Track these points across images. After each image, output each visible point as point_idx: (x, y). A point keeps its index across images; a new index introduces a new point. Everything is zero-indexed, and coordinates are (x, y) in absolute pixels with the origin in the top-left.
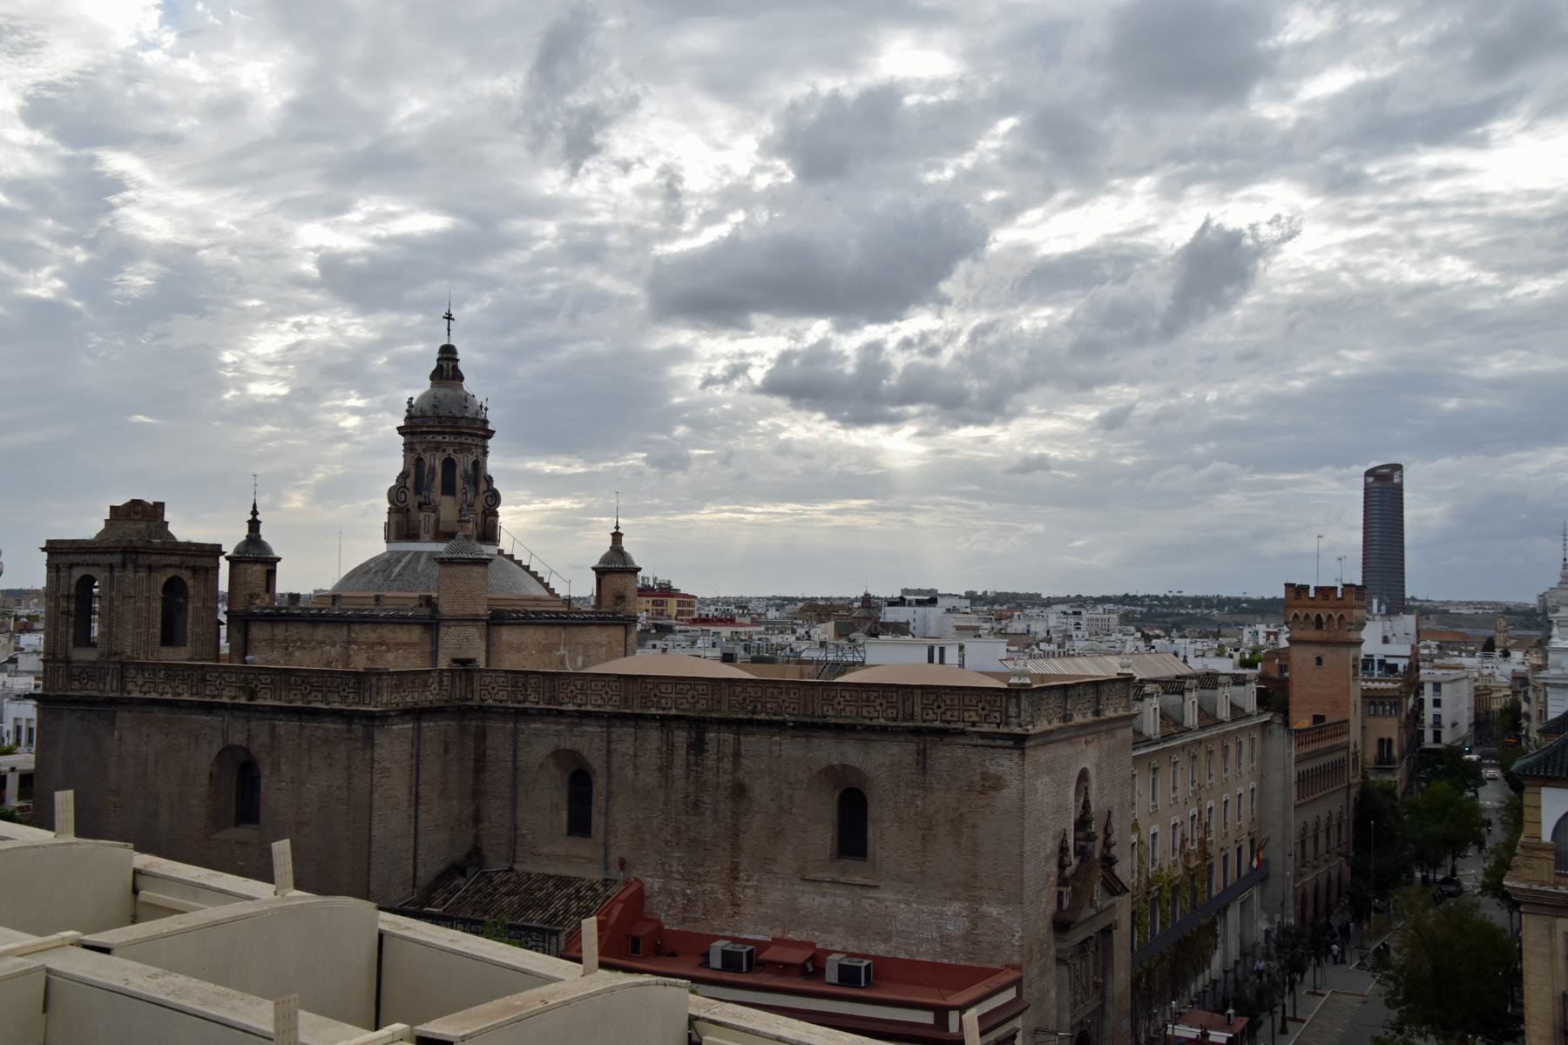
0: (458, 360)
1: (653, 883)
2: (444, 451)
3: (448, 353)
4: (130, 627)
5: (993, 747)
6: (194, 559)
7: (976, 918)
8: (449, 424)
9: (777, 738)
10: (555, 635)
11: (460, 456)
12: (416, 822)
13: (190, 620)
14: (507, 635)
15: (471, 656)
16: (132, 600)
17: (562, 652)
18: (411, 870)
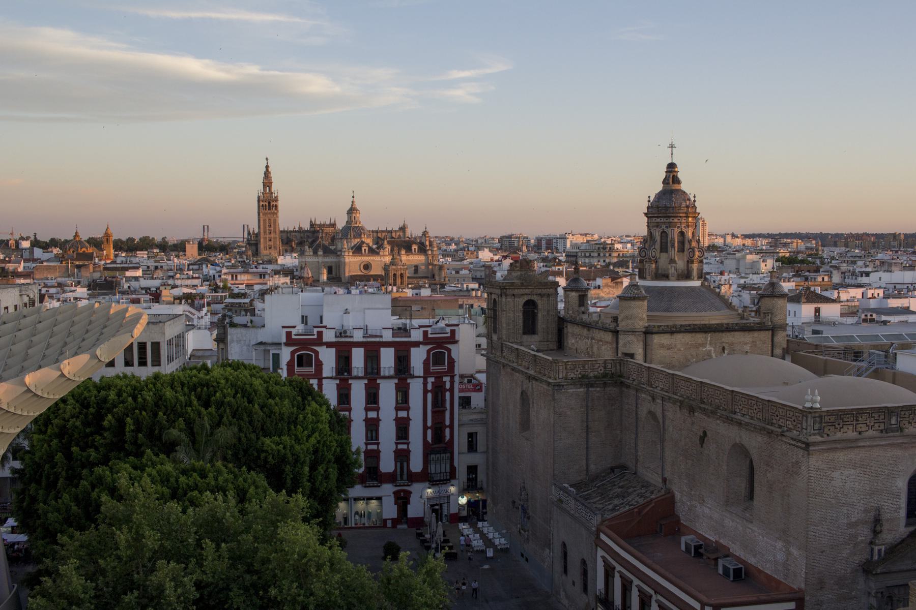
0: (677, 172)
1: (678, 496)
2: (661, 227)
3: (671, 167)
4: (504, 326)
5: (797, 447)
6: (540, 290)
7: (788, 554)
8: (663, 211)
9: (718, 422)
10: (700, 338)
11: (669, 230)
12: (587, 441)
13: (540, 321)
14: (657, 339)
15: (631, 351)
16: (505, 312)
17: (708, 348)
18: (585, 467)
